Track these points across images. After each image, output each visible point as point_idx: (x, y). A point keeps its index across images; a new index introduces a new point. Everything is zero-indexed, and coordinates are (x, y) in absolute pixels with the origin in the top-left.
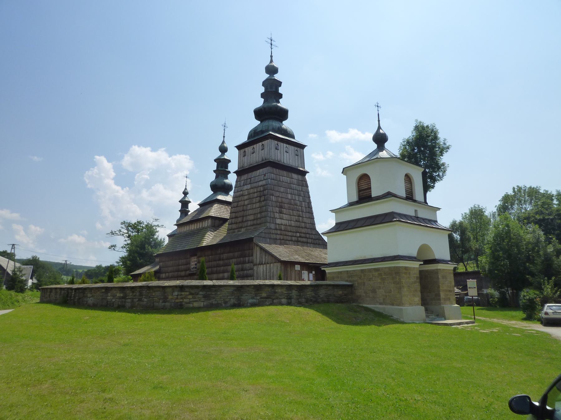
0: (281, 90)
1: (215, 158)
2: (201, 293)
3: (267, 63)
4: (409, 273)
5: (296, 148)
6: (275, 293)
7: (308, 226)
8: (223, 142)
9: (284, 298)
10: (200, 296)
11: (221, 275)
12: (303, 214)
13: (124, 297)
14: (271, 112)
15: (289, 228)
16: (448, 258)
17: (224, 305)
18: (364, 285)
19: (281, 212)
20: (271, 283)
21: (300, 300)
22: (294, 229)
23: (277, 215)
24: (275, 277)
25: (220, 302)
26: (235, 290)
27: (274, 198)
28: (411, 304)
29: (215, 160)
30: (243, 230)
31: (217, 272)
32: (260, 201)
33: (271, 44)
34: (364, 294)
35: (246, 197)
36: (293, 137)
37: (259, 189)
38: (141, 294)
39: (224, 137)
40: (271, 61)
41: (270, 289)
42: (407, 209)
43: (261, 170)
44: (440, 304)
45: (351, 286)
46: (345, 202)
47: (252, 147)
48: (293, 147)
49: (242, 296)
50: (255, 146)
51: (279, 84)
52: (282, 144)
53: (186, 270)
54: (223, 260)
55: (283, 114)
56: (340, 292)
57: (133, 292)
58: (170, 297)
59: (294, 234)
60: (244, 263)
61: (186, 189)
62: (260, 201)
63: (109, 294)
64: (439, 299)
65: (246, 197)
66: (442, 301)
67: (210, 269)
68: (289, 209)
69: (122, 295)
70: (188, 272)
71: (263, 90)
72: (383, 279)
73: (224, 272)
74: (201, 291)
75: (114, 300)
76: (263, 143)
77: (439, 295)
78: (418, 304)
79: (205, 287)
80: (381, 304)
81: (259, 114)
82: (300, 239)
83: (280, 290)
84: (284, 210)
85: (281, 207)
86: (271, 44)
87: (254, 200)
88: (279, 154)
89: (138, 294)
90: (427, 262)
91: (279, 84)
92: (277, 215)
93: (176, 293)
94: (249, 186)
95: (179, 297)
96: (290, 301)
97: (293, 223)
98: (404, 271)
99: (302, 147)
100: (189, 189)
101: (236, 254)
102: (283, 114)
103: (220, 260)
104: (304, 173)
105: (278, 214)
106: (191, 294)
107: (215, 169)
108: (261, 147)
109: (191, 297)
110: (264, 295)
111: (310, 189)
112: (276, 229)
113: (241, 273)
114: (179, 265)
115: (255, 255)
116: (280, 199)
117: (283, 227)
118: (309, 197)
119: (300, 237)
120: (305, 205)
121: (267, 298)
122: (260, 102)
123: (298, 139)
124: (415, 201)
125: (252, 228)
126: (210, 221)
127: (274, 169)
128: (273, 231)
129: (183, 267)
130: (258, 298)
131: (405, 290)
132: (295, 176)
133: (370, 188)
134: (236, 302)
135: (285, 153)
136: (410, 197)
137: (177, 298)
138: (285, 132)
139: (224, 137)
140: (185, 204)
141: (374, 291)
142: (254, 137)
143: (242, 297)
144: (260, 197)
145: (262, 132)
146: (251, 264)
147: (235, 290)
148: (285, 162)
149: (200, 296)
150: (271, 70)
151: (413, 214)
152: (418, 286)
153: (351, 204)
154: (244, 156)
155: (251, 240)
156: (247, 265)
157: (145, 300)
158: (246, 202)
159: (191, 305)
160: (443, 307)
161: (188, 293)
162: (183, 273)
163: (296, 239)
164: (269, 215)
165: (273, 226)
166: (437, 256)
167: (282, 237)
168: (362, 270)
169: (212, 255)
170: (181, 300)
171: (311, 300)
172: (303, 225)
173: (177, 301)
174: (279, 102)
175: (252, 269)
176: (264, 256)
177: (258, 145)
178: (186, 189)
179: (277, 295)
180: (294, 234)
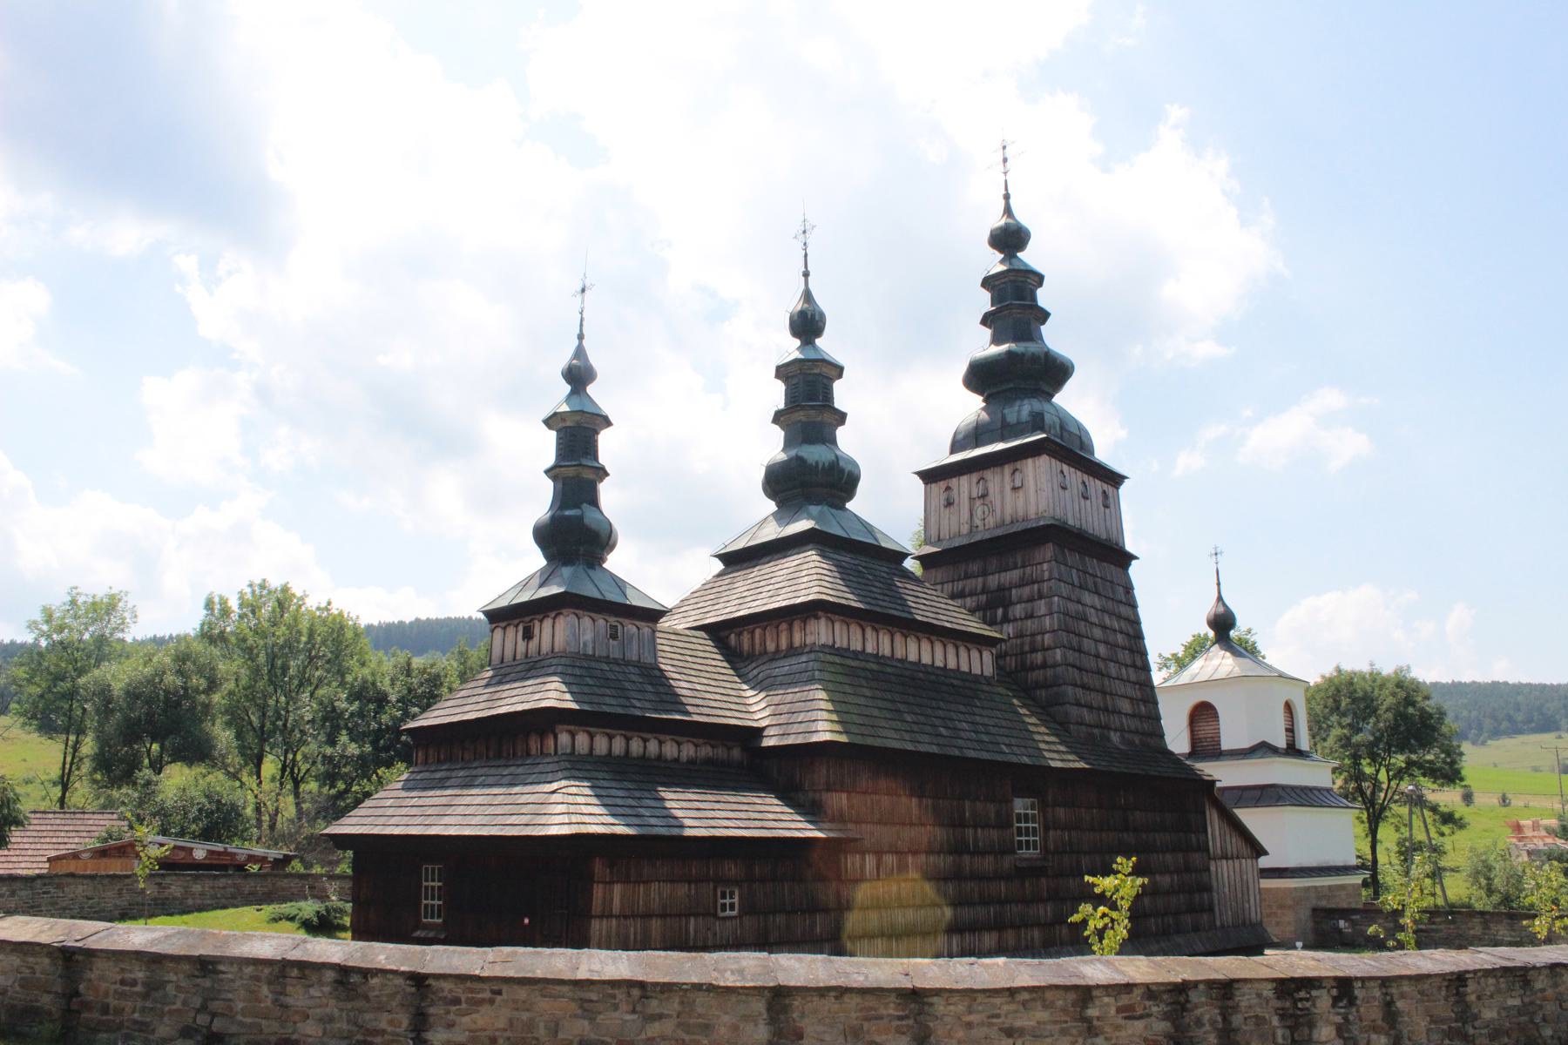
39: (806, 275)
40: (1008, 211)
61: (580, 352)
70: (1007, 862)
139: (806, 275)
150: (1010, 239)
168: (1330, 887)
178: (580, 352)
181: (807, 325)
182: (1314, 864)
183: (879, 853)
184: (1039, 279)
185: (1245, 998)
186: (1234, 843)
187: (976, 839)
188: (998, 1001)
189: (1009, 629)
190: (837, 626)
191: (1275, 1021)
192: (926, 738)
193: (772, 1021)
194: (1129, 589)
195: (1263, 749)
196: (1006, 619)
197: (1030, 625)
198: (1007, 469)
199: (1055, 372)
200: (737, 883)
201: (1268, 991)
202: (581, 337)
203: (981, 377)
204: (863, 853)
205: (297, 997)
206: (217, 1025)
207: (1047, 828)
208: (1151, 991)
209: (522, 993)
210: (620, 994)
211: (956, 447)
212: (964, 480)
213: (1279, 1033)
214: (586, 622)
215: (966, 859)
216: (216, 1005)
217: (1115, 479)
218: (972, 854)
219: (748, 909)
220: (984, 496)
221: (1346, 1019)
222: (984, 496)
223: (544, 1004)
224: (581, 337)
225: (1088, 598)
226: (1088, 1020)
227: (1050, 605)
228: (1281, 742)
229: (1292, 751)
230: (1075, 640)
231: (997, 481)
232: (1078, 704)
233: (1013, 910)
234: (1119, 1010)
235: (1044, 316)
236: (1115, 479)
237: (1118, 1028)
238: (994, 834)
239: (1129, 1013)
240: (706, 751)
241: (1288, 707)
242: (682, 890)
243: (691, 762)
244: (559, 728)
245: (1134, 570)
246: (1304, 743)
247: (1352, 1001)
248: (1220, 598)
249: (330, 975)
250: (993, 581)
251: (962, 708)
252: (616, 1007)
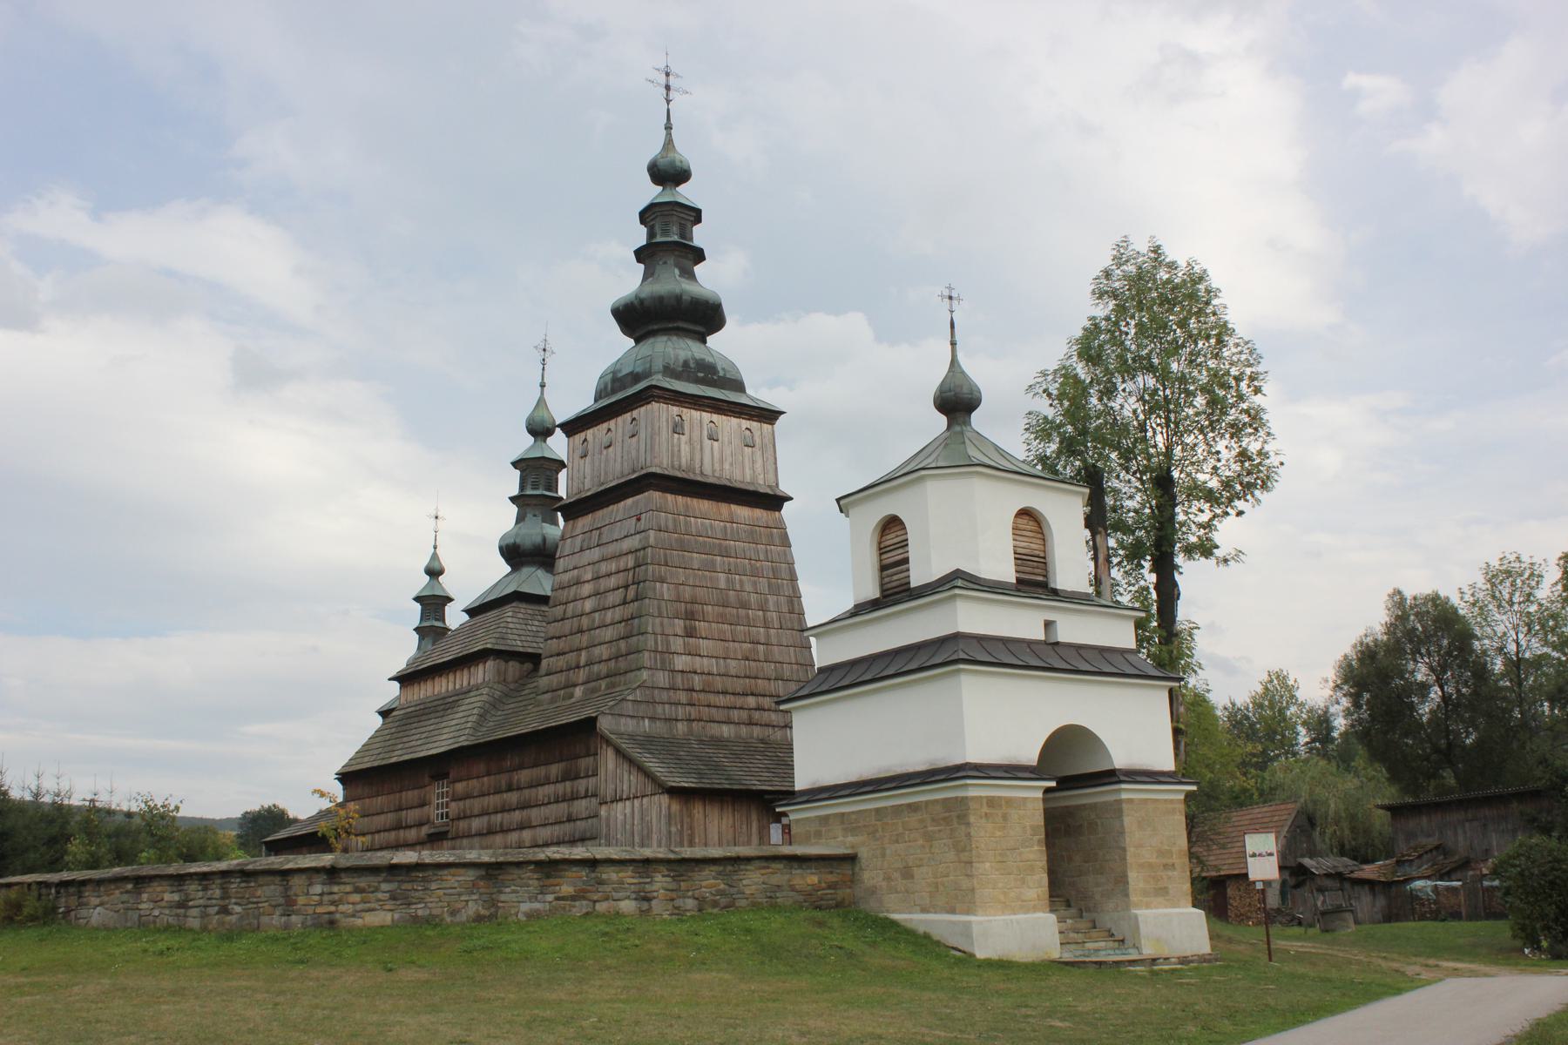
0: (700, 236)
1: (515, 457)
2: (384, 886)
3: (653, 150)
4: (1005, 817)
5: (745, 423)
6: (601, 882)
7: (787, 671)
8: (541, 402)
9: (628, 898)
10: (380, 895)
11: (513, 837)
12: (768, 636)
13: (182, 905)
14: (669, 313)
15: (719, 683)
16: (1167, 762)
17: (449, 919)
18: (883, 855)
19: (690, 633)
20: (587, 855)
21: (679, 902)
22: (739, 685)
23: (677, 644)
24: (655, 837)
25: (435, 912)
26: (482, 878)
27: (665, 591)
28: (1006, 907)
29: (515, 464)
30: (578, 692)
33: (668, 88)
34: (884, 884)
35: (587, 589)
36: (739, 386)
37: (622, 564)
38: (225, 896)
39: (543, 386)
40: (669, 143)
41: (583, 873)
42: (1022, 622)
43: (629, 501)
44: (1127, 908)
45: (851, 859)
46: (849, 605)
47: (605, 426)
48: (734, 421)
49: (500, 892)
50: (612, 424)
51: (696, 215)
52: (696, 414)
53: (420, 825)
54: (519, 789)
55: (705, 317)
56: (813, 879)
57: (205, 889)
58: (301, 900)
59: (739, 701)
60: (574, 797)
61: (435, 557)
62: (625, 603)
63: (145, 896)
64: (1127, 895)
65: (587, 589)
66: (1134, 898)
67: (486, 818)
68: (722, 619)
69: (176, 897)
70: (425, 830)
71: (640, 236)
72: (929, 838)
74: (385, 881)
75: (156, 913)
76: (635, 413)
77: (1122, 880)
78: (1035, 909)
79: (393, 869)
80: (924, 910)
81: (635, 318)
82: (756, 715)
83: (614, 876)
84: (701, 626)
85: (690, 616)
86: (668, 88)
88: (685, 449)
89: (218, 893)
90: (1068, 782)
91: (696, 215)
92: (677, 644)
93: (318, 889)
94: (595, 554)
95: (326, 898)
96: (645, 906)
97: (733, 666)
98: (985, 809)
99: (769, 415)
100: (445, 561)
101: (555, 770)
102: (705, 317)
103: (510, 789)
104: (774, 501)
105: (680, 641)
106: (358, 890)
107: (515, 491)
108: (629, 427)
109: (356, 897)
110: (567, 889)
111: (797, 551)
112: (673, 688)
113: (568, 827)
115: (602, 772)
116: (687, 592)
117: (697, 681)
118: (793, 578)
119: (759, 708)
120: (777, 604)
121: (573, 898)
122: (629, 281)
123: (758, 392)
124: (1055, 592)
125: (603, 684)
126: (490, 664)
127: (670, 497)
128: (665, 696)
129: (412, 815)
130: (550, 898)
131: (985, 867)
132: (743, 512)
133: (906, 561)
134: (483, 912)
135: (707, 442)
136: (1034, 582)
137: (320, 904)
138: (707, 372)
139: (543, 386)
140: (433, 604)
141: (907, 873)
142: (614, 392)
143: (503, 897)
144: (626, 587)
145: (635, 377)
146: (593, 800)
147: (482, 878)
148: (707, 469)
149: (380, 895)
150: (668, 174)
151: (1038, 634)
152: (1036, 854)
153: (859, 610)
154: (584, 456)
155: (591, 722)
156: (581, 806)
157: (238, 909)
158: (588, 605)
159: (359, 922)
160: (1136, 917)
161: (348, 888)
162: (412, 834)
163: (744, 715)
164: (651, 644)
165: (662, 678)
166: (1120, 759)
167: (693, 712)
168: (877, 810)
169: (489, 774)
170: (332, 908)
171: (715, 904)
172: (770, 669)
173: (319, 910)
174: (691, 276)
175: (596, 816)
177: (620, 419)
178: (435, 557)
179: (608, 888)
180: (739, 701)
182: (853, 778)
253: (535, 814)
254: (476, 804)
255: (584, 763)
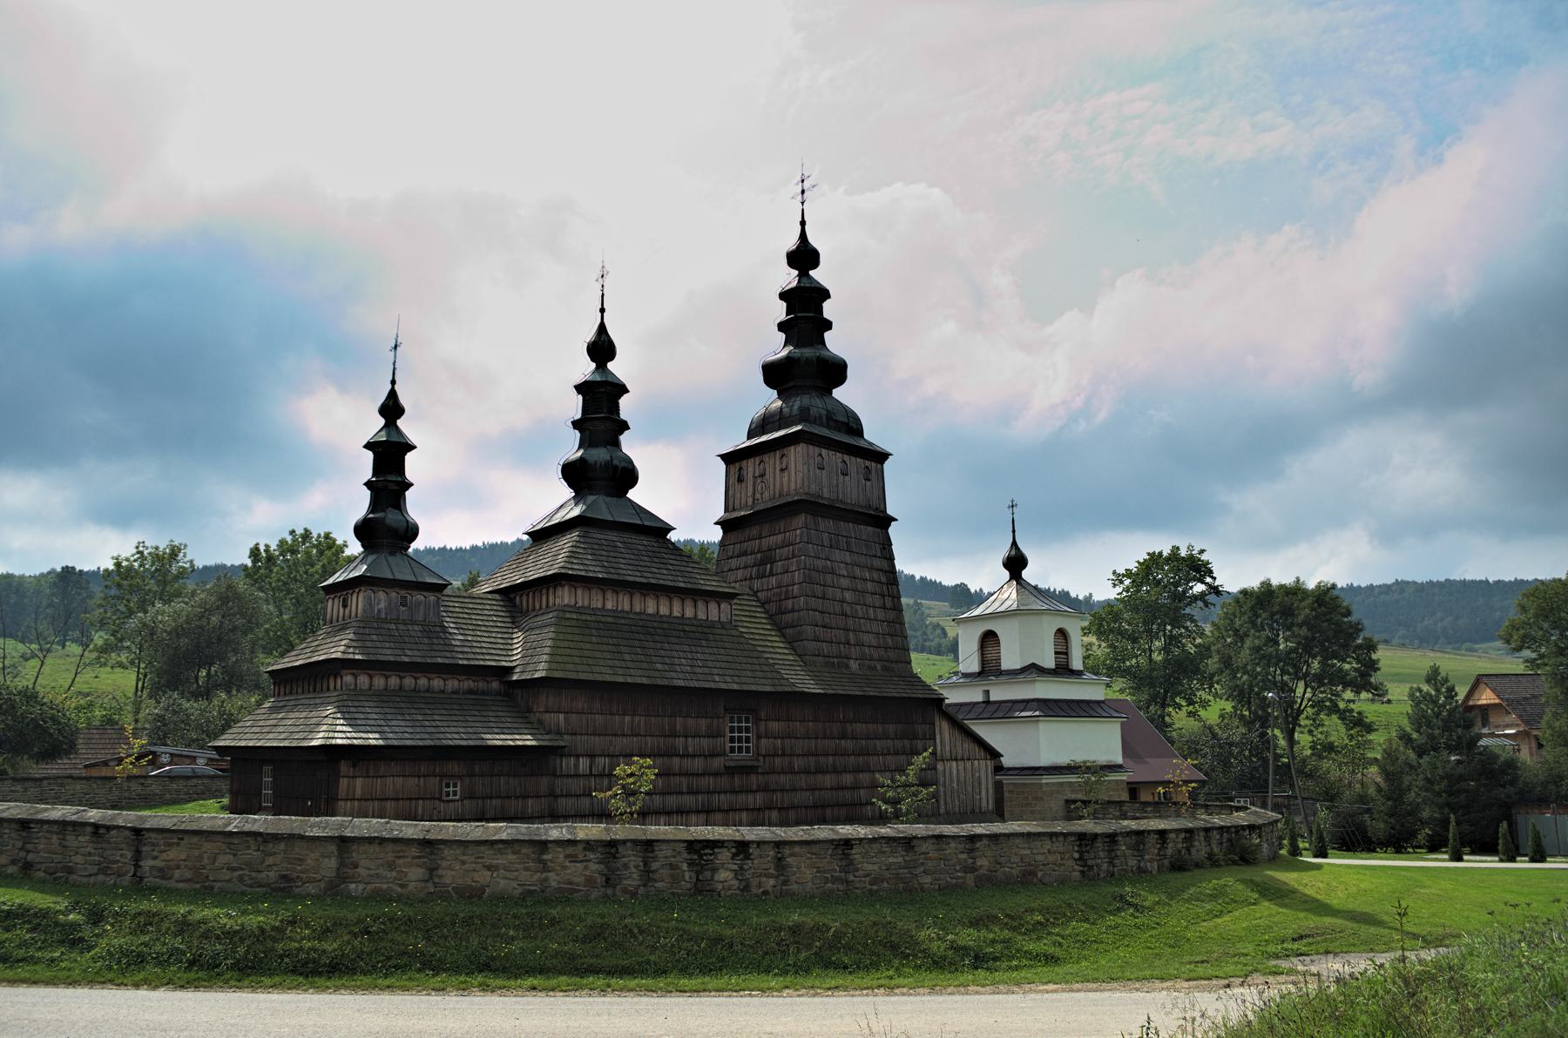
31: (835, 771)
32: (884, 608)
39: (602, 310)
40: (803, 236)
53: (713, 755)
61: (393, 394)
70: (717, 763)
73: (858, 770)
87: (869, 599)
101: (892, 728)
103: (844, 737)
114: (674, 735)
139: (602, 310)
150: (804, 257)
162: (698, 764)
169: (816, 720)
176: (959, 744)
181: (601, 349)
183: (592, 756)
184: (825, 294)
185: (663, 852)
186: (969, 746)
187: (686, 747)
188: (482, 848)
189: (773, 580)
190: (579, 592)
191: (685, 866)
192: (639, 672)
193: (340, 856)
194: (887, 544)
195: (1034, 669)
196: (771, 574)
197: (786, 579)
198: (778, 454)
199: (836, 372)
200: (460, 777)
201: (681, 847)
202: (393, 382)
203: (774, 374)
204: (578, 756)
205: (71, 840)
206: (30, 857)
207: (759, 737)
208: (589, 845)
209: (195, 839)
210: (251, 841)
211: (750, 436)
212: (751, 461)
213: (687, 875)
214: (382, 595)
215: (676, 760)
216: (29, 846)
217: (882, 457)
218: (682, 756)
219: (470, 795)
220: (762, 476)
221: (741, 868)
222: (762, 476)
223: (207, 846)
224: (393, 382)
225: (837, 555)
226: (544, 862)
227: (798, 563)
228: (1049, 662)
229: (1063, 670)
230: (818, 590)
231: (772, 462)
232: (817, 639)
233: (723, 800)
234: (567, 857)
235: (828, 325)
236: (882, 457)
237: (565, 868)
238: (705, 742)
239: (573, 858)
240: (469, 684)
241: (1062, 634)
242: (413, 781)
243: (455, 692)
244: (344, 672)
245: (893, 530)
246: (1077, 664)
247: (748, 857)
248: (1014, 543)
249: (89, 829)
250: (765, 543)
251: (686, 648)
252: (249, 848)
253: (872, 760)
254: (800, 745)
255: (920, 729)
